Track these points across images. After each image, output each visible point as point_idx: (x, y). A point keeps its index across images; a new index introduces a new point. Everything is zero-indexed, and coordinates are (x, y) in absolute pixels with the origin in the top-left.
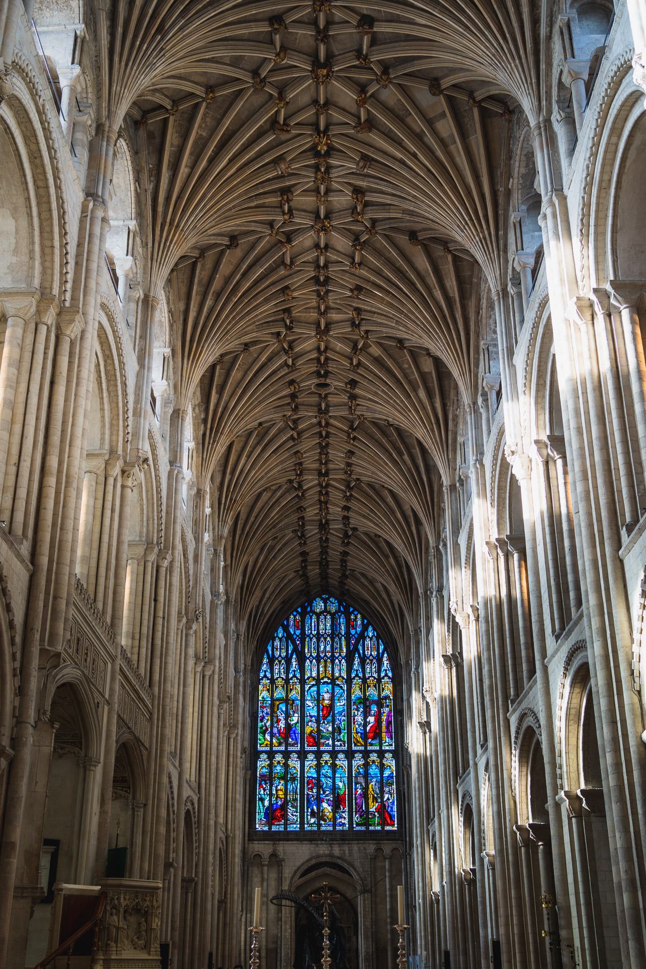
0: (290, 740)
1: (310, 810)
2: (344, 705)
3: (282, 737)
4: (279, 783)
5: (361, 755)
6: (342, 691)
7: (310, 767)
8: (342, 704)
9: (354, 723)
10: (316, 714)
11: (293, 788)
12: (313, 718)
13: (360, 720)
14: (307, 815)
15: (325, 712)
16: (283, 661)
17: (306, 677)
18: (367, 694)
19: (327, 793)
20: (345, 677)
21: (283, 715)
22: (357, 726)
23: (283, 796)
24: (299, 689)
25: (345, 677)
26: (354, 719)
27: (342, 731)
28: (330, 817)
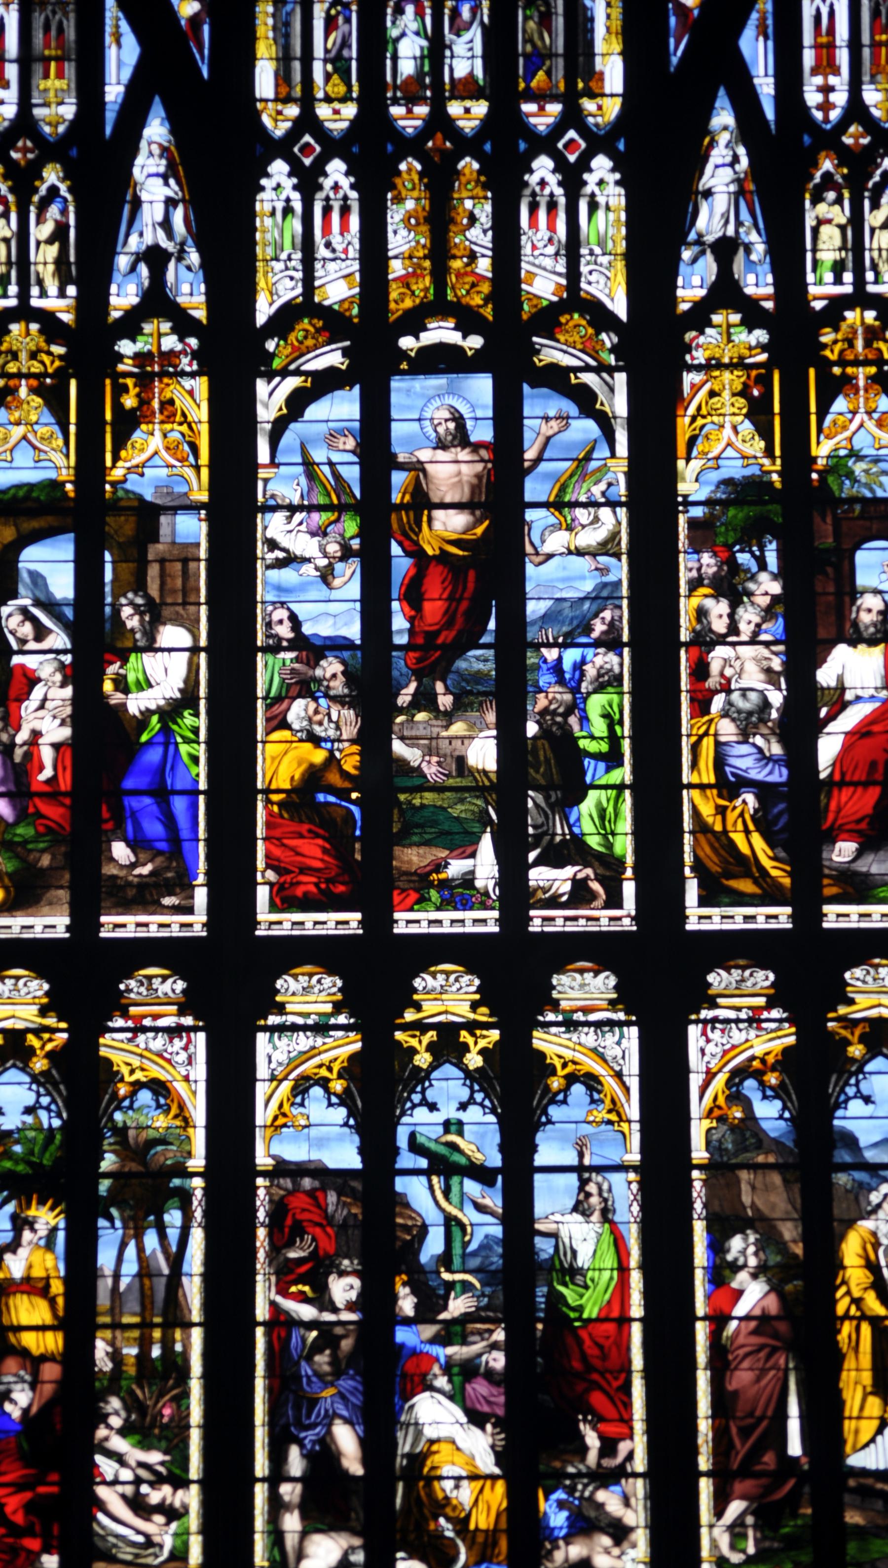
0: (120, 851)
1: (296, 1463)
2: (608, 547)
3: (51, 832)
4: (20, 1223)
5: (764, 978)
6: (587, 428)
7: (302, 1087)
8: (589, 538)
9: (701, 706)
10: (353, 631)
11: (145, 1271)
12: (331, 667)
13: (753, 678)
14: (276, 1505)
15: (434, 610)
16: (52, 175)
17: (263, 311)
18: (822, 450)
19: (458, 1306)
20: (620, 307)
21: (59, 639)
22: (727, 729)
23: (53, 1342)
24: (201, 414)
25: (620, 307)
26: (700, 671)
27: (594, 771)
28: (482, 1520)
